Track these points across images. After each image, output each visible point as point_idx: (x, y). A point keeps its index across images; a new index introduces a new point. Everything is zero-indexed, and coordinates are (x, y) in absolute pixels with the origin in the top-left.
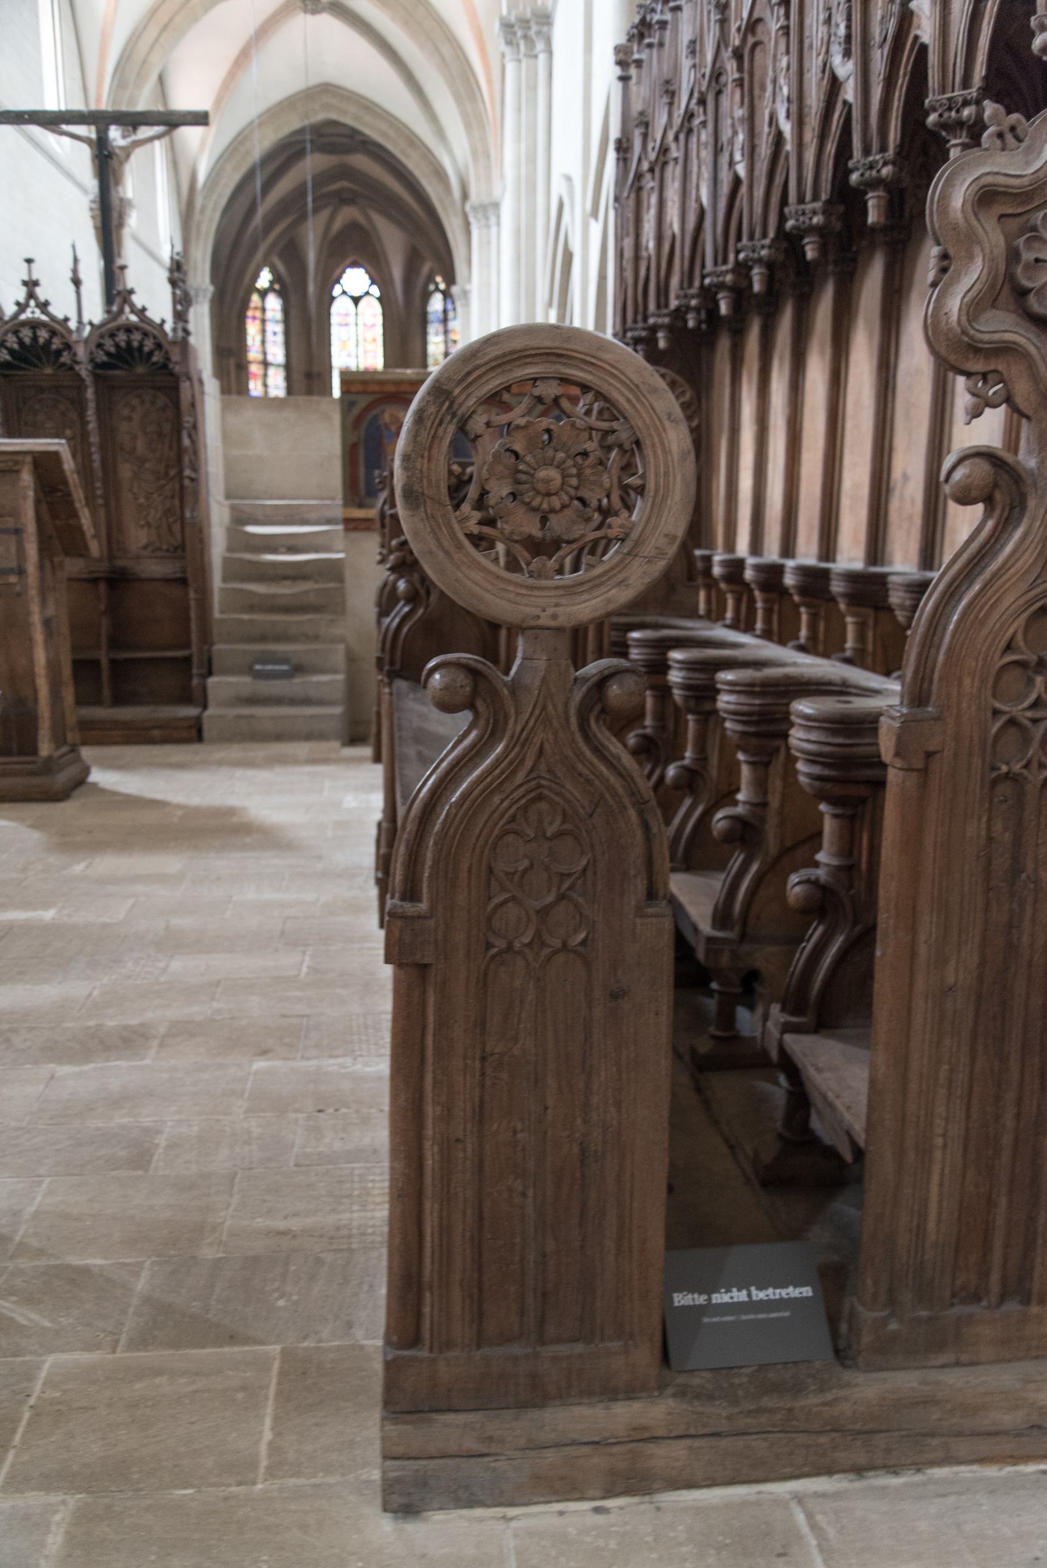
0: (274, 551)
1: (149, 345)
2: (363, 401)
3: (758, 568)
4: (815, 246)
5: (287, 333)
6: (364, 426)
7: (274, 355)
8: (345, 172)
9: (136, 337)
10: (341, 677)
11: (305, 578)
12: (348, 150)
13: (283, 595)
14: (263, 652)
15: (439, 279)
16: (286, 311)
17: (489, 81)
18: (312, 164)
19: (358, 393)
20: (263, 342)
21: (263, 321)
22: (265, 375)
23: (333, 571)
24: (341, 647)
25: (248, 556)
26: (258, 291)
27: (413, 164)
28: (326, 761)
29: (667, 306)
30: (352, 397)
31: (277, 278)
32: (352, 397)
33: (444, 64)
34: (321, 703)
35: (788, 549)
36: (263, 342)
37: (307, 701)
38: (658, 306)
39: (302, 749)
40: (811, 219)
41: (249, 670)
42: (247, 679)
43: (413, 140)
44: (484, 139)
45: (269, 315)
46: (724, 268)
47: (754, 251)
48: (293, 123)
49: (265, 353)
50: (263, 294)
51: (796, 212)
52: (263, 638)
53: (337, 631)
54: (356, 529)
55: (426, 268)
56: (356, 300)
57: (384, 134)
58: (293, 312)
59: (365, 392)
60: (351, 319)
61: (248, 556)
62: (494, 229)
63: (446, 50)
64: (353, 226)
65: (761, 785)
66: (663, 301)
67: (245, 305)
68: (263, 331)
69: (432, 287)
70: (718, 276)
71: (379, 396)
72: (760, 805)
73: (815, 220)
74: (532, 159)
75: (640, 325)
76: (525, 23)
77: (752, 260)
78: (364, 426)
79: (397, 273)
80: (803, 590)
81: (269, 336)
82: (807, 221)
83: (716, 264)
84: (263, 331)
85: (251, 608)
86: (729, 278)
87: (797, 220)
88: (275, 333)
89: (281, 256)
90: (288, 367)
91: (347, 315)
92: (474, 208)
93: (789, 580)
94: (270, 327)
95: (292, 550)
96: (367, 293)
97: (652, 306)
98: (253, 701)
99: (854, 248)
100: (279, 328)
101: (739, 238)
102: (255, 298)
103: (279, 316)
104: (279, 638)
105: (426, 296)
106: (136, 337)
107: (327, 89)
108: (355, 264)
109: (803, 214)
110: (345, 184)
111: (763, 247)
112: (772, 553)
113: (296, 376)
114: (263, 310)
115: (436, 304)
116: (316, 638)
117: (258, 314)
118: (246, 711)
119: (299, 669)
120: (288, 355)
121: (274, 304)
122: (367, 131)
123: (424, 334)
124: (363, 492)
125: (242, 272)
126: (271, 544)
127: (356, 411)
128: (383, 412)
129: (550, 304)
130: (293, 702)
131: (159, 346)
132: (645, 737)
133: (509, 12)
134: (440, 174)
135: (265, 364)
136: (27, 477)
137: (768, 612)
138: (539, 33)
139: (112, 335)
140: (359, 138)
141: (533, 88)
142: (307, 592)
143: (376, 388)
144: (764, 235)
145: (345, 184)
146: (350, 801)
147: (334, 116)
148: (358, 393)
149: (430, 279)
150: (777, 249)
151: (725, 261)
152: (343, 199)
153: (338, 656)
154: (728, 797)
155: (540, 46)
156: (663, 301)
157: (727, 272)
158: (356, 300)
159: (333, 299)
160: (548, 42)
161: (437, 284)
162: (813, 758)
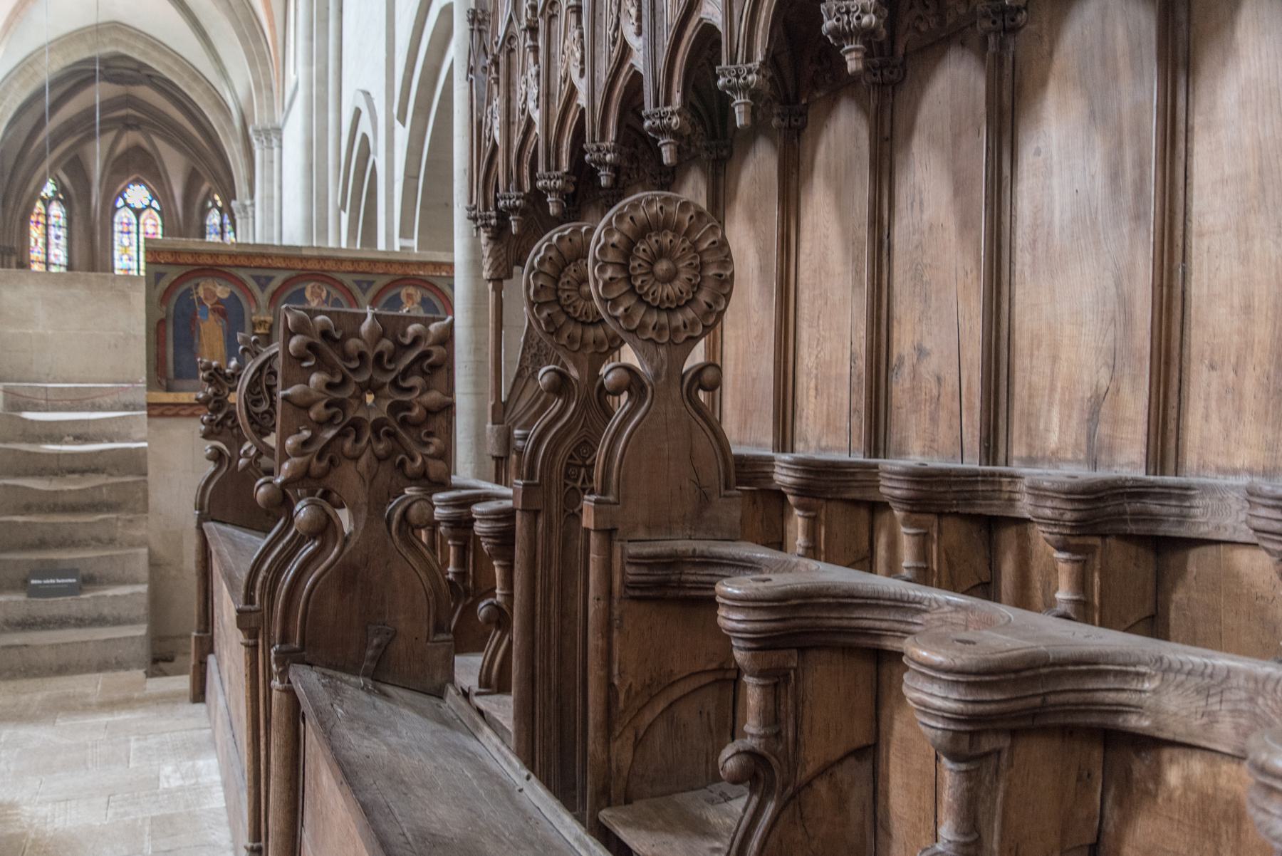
0: (59, 440)
2: (173, 274)
4: (860, 55)
5: (70, 239)
6: (174, 300)
7: (56, 256)
8: (130, 101)
10: (143, 588)
11: (96, 471)
12: (134, 82)
13: (70, 491)
14: (42, 562)
15: (217, 197)
16: (69, 219)
17: (272, 26)
18: (98, 93)
19: (167, 264)
20: (47, 245)
21: (47, 226)
23: (134, 463)
24: (144, 551)
25: (25, 447)
26: (43, 200)
27: (196, 95)
28: (127, 703)
29: (557, 168)
30: (161, 269)
31: (62, 188)
32: (161, 269)
34: (118, 622)
36: (47, 245)
37: (100, 621)
38: (548, 169)
39: (91, 685)
40: (858, 18)
41: (23, 585)
42: (20, 597)
43: (197, 76)
44: (267, 74)
45: (52, 220)
46: (669, 109)
47: (738, 77)
48: (82, 52)
49: (47, 254)
50: (47, 202)
51: (838, 10)
52: (42, 544)
53: (138, 533)
54: (162, 415)
55: (205, 188)
56: (138, 213)
57: (169, 68)
58: (76, 219)
59: (176, 264)
60: (133, 228)
61: (25, 447)
62: (276, 150)
64: (137, 149)
66: (553, 163)
67: (29, 210)
68: (47, 235)
69: (210, 204)
70: (661, 118)
71: (191, 268)
73: (865, 20)
74: (323, 81)
75: (513, 193)
77: (734, 89)
78: (174, 300)
79: (178, 190)
80: (803, 491)
81: (52, 240)
82: (854, 21)
83: (657, 105)
84: (47, 235)
85: (27, 509)
86: (675, 120)
87: (838, 20)
88: (58, 237)
89: (64, 170)
91: (129, 224)
92: (257, 132)
94: (53, 231)
95: (79, 439)
96: (149, 206)
98: (26, 624)
99: (804, 101)
100: (62, 233)
102: (39, 204)
103: (62, 222)
104: (62, 544)
105: (204, 212)
107: (116, 27)
108: (137, 181)
109: (848, 12)
110: (131, 111)
111: (750, 72)
114: (47, 216)
116: (111, 541)
117: (42, 219)
118: (18, 638)
119: (89, 581)
121: (57, 210)
122: (154, 66)
124: (171, 374)
125: (27, 181)
126: (53, 433)
127: (165, 283)
128: (197, 285)
129: (343, 207)
130: (81, 623)
132: (750, 753)
140: (145, 72)
142: (100, 487)
143: (191, 260)
144: (749, 59)
145: (131, 111)
146: (170, 775)
147: (122, 50)
148: (167, 264)
149: (208, 196)
150: (764, 76)
151: (668, 102)
152: (127, 124)
153: (141, 566)
156: (553, 163)
157: (673, 113)
158: (138, 213)
159: (115, 210)
161: (215, 202)
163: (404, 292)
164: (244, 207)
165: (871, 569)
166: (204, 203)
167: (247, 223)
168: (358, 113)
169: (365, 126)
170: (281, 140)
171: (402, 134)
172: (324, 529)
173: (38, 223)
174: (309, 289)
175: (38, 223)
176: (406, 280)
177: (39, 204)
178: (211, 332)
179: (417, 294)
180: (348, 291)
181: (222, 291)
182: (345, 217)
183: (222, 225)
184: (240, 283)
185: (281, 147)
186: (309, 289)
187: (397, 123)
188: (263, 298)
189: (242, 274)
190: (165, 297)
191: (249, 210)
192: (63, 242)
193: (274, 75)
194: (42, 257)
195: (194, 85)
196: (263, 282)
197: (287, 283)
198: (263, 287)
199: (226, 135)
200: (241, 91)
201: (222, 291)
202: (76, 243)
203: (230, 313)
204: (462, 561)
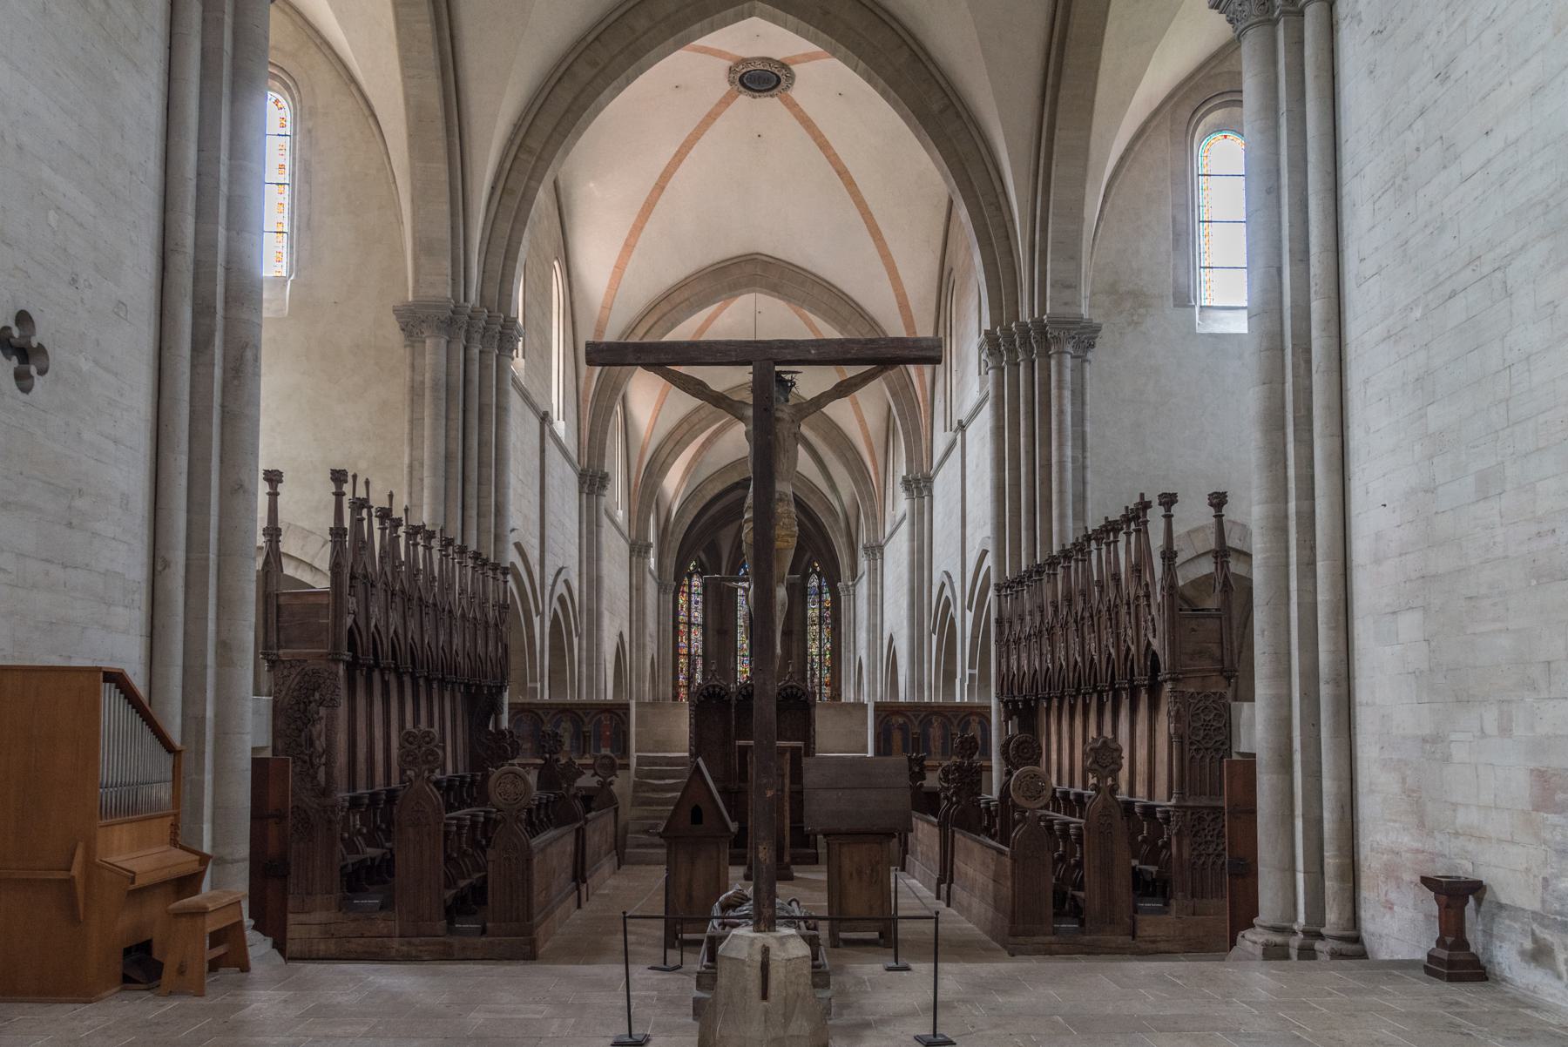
1: (800, 693)
2: (884, 714)
3: (1060, 792)
5: (705, 602)
9: (795, 690)
17: (877, 474)
21: (690, 594)
22: (690, 632)
31: (700, 564)
33: (847, 464)
35: (1072, 784)
43: (814, 489)
44: (873, 506)
45: (694, 589)
49: (690, 616)
50: (690, 576)
55: (806, 558)
63: (849, 455)
65: (1065, 847)
68: (689, 601)
72: (1065, 851)
74: (921, 551)
76: (917, 481)
80: (1076, 800)
81: (693, 605)
84: (689, 601)
88: (697, 603)
89: (704, 551)
90: (704, 626)
93: (1072, 797)
97: (1016, 693)
101: (1050, 689)
103: (700, 590)
106: (795, 690)
112: (1066, 786)
113: (710, 633)
115: (814, 582)
117: (686, 589)
120: (705, 618)
123: (805, 603)
127: (880, 718)
131: (804, 694)
133: (908, 474)
134: (830, 509)
135: (690, 624)
136: (788, 755)
137: (1065, 808)
138: (924, 486)
139: (785, 689)
141: (921, 514)
149: (810, 564)
154: (1057, 850)
155: (925, 493)
160: (930, 491)
161: (814, 570)
162: (1075, 835)
163: (971, 718)
164: (848, 587)
165: (1075, 817)
166: (807, 569)
167: (849, 600)
168: (943, 585)
169: (947, 592)
170: (882, 554)
171: (970, 616)
172: (958, 802)
173: (683, 592)
174: (934, 718)
175: (683, 592)
176: (971, 714)
177: (686, 579)
178: (897, 737)
179: (977, 719)
180: (949, 719)
181: (901, 720)
182: (935, 638)
183: (820, 587)
184: (908, 717)
185: (882, 559)
186: (934, 718)
187: (967, 611)
188: (917, 723)
189: (909, 713)
190: (881, 722)
191: (851, 588)
192: (700, 606)
193: (877, 508)
194: (685, 619)
195: (811, 496)
196: (916, 717)
197: (925, 716)
198: (916, 718)
199: (833, 532)
200: (846, 499)
201: (901, 720)
202: (709, 610)
203: (903, 728)
204: (989, 821)
